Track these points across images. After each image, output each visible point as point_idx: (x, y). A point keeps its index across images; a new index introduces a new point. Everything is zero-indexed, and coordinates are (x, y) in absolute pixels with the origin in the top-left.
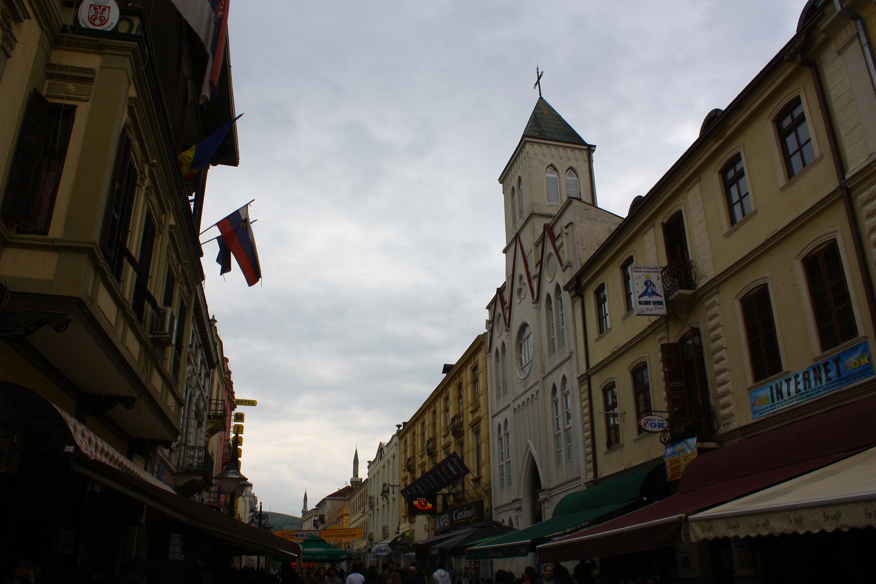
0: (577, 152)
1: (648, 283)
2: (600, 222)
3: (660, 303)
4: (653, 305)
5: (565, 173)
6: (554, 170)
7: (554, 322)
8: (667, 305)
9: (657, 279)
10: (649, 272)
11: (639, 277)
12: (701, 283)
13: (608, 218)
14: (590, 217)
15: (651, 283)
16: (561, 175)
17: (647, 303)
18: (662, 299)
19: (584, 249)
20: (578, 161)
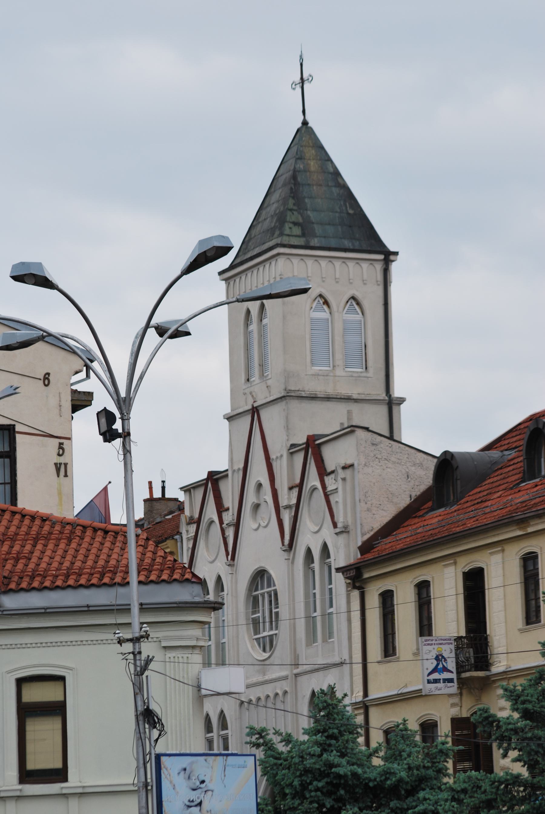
0: (365, 265)
1: (439, 658)
2: (394, 463)
3: (450, 681)
4: (443, 683)
5: (341, 309)
6: (324, 303)
7: (317, 591)
8: (459, 683)
9: (449, 652)
10: (441, 644)
11: (430, 651)
12: (495, 669)
13: (406, 456)
14: (379, 457)
15: (443, 657)
16: (336, 315)
17: (436, 681)
18: (454, 676)
19: (368, 510)
20: (365, 284)
